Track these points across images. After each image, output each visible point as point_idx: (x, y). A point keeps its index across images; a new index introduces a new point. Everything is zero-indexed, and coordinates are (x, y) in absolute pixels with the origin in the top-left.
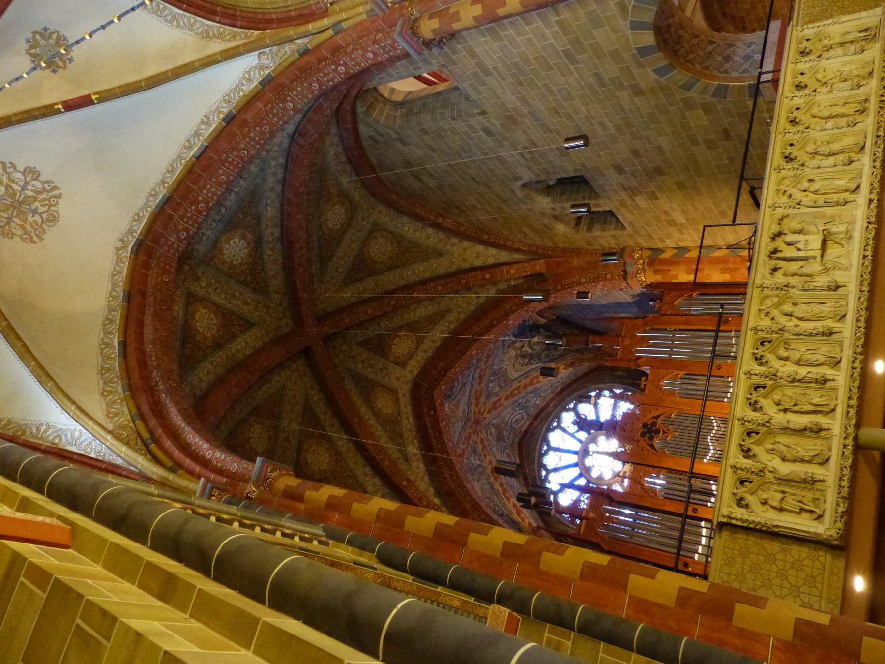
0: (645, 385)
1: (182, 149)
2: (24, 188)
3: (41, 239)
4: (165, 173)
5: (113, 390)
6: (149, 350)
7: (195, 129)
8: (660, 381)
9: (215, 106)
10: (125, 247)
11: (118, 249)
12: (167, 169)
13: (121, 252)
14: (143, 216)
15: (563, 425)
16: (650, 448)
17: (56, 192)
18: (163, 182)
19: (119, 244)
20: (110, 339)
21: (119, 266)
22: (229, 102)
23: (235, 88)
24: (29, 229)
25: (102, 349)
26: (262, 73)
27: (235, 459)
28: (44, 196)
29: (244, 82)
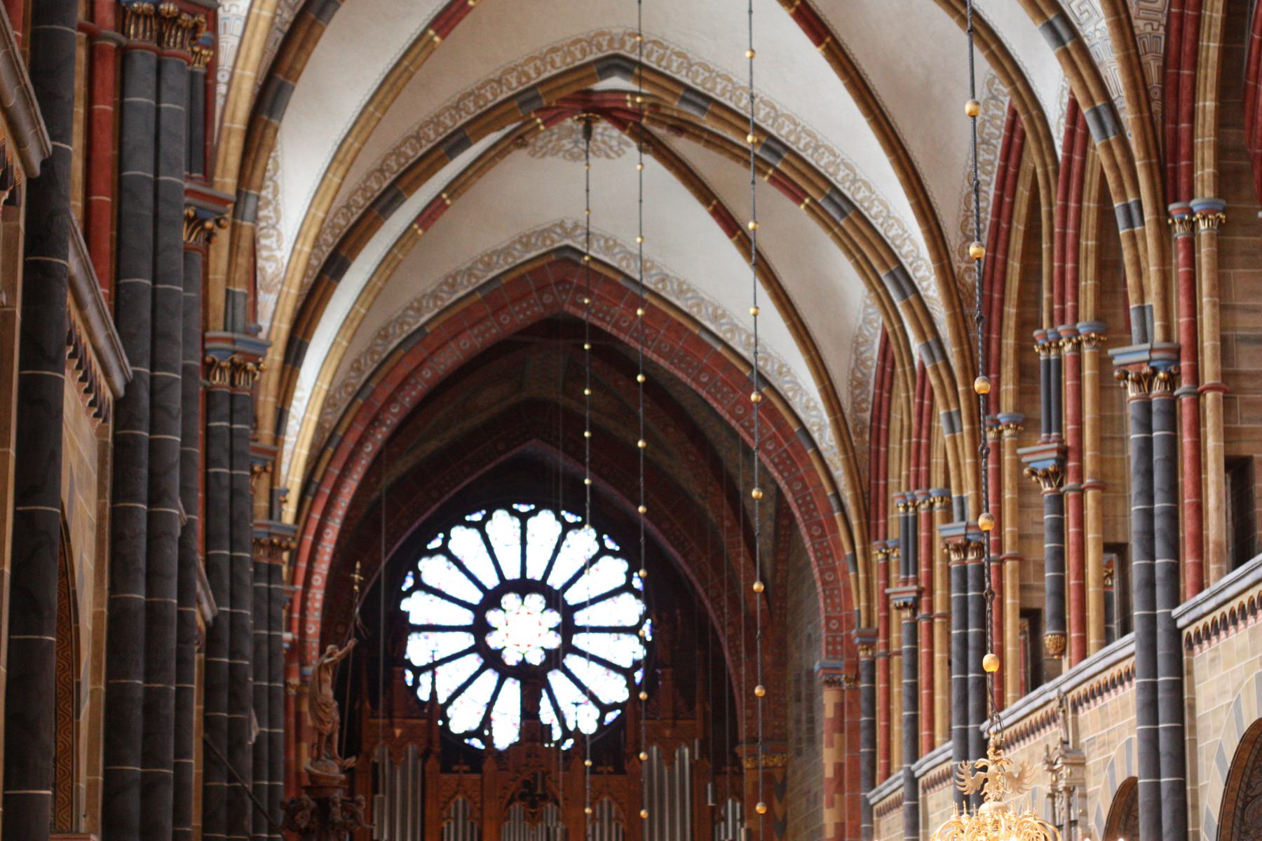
0: (601, 773)
1: (713, 304)
2: (602, 134)
3: (544, 155)
4: (678, 280)
5: (362, 368)
6: (424, 373)
7: (741, 325)
8: (610, 794)
9: (774, 354)
10: (567, 234)
11: (561, 225)
12: (684, 282)
13: (558, 230)
14: (614, 255)
15: (570, 534)
16: (508, 796)
17: (612, 155)
18: (664, 279)
19: (569, 225)
20: (428, 307)
21: (537, 240)
22: (780, 373)
23: (797, 384)
24: (550, 146)
25: (411, 307)
26: (815, 428)
27: (319, 626)
28: (602, 146)
29: (804, 399)
